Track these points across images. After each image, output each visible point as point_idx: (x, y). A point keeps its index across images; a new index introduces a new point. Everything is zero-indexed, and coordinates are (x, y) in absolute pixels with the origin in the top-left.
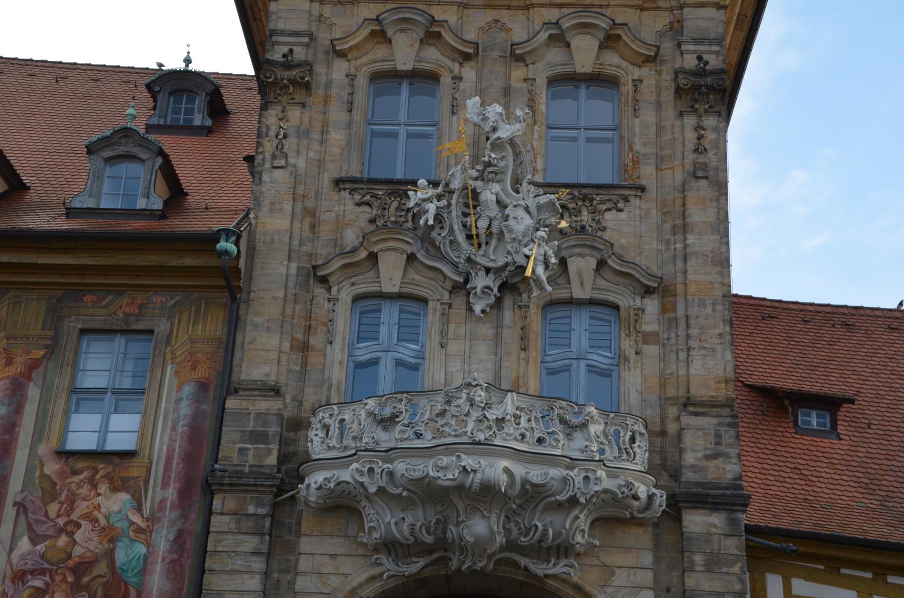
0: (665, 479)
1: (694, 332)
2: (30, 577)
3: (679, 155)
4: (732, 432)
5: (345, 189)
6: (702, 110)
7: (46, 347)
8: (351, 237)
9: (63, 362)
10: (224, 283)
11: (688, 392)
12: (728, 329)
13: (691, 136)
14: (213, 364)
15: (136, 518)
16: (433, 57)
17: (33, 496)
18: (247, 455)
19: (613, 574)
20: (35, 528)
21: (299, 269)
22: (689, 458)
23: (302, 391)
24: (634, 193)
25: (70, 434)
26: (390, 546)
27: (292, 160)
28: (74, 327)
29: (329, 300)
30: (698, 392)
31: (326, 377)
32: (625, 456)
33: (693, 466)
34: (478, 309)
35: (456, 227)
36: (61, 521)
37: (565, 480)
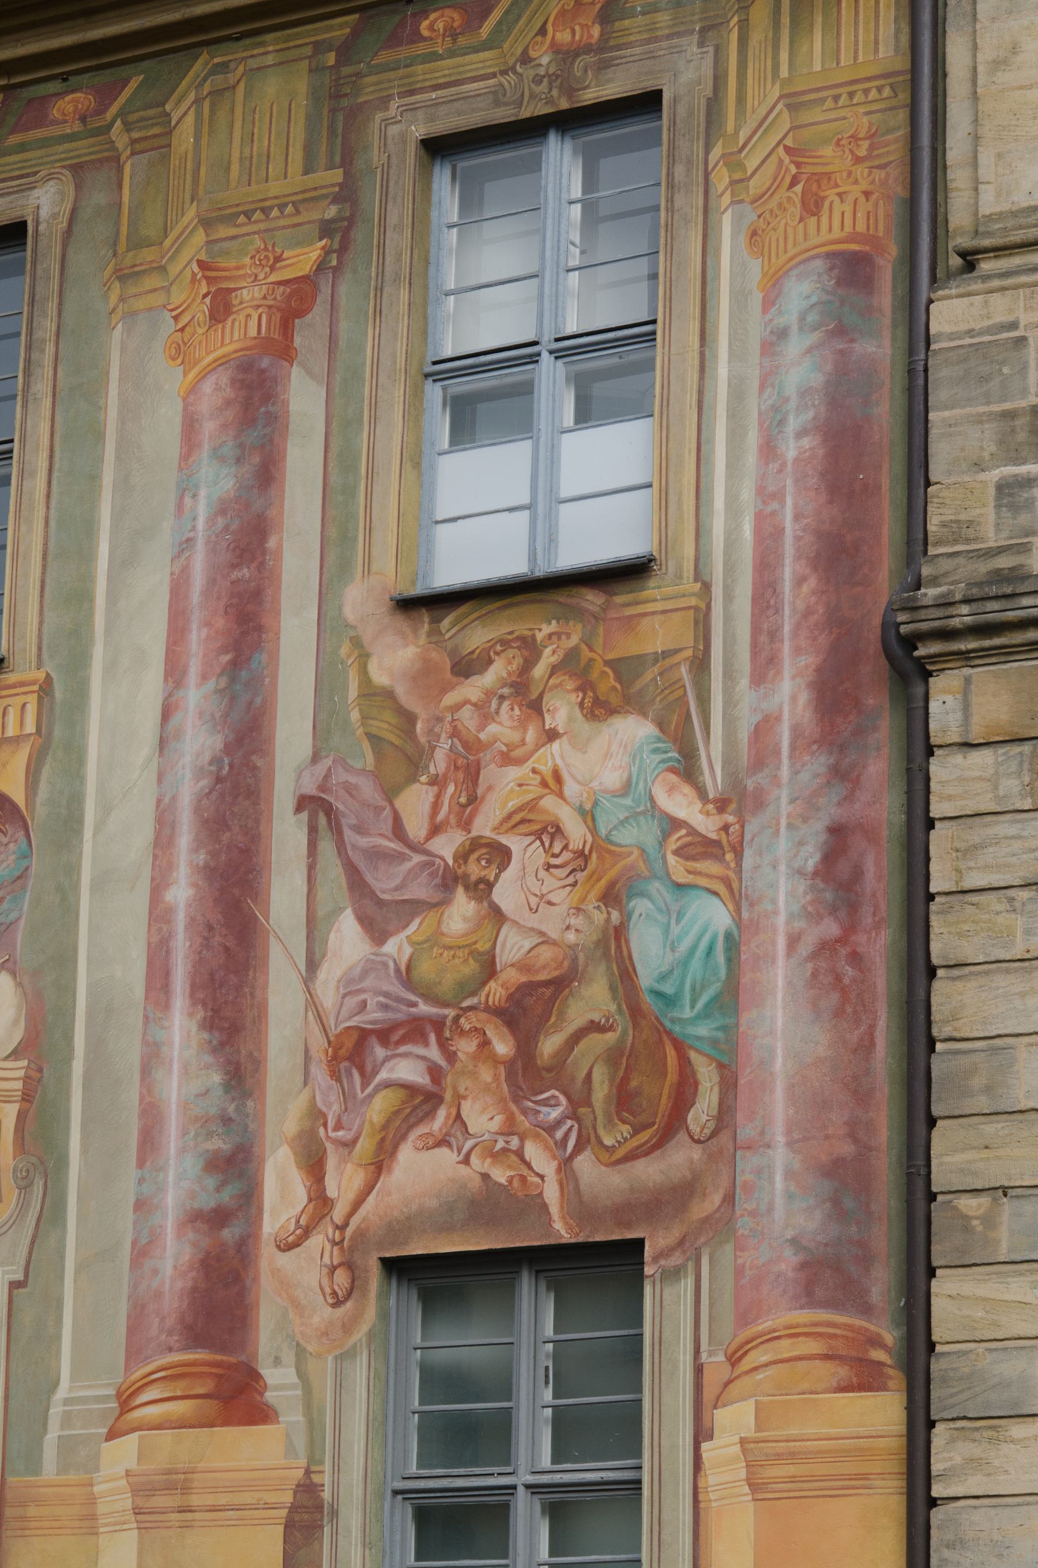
2: (380, 1052)
7: (326, 229)
9: (381, 273)
14: (879, 175)
15: (682, 805)
17: (348, 769)
20: (369, 878)
28: (403, 138)
36: (446, 847)
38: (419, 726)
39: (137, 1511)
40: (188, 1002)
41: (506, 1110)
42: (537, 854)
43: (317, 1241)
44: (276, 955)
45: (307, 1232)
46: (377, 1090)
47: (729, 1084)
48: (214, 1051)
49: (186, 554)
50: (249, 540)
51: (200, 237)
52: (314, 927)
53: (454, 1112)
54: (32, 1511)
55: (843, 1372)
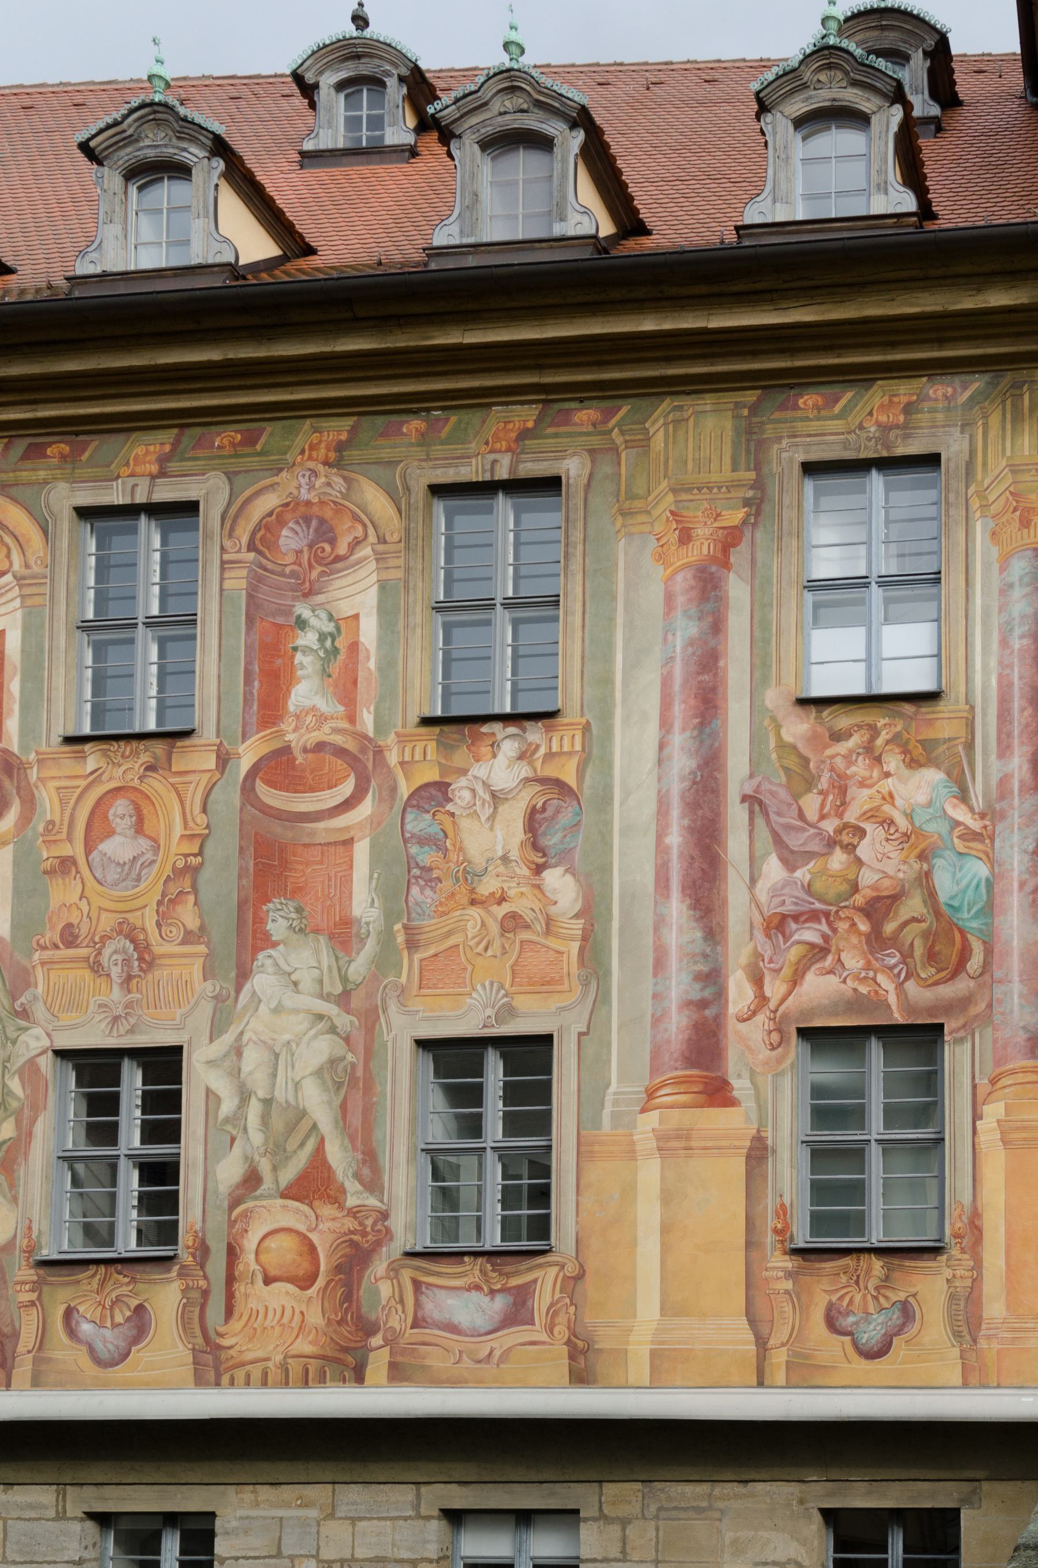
2: (794, 926)
17: (771, 783)
20: (785, 838)
36: (829, 826)
38: (811, 765)
39: (660, 1149)
40: (680, 895)
41: (866, 958)
42: (881, 833)
43: (760, 1018)
44: (731, 873)
45: (754, 1013)
46: (793, 944)
48: (697, 920)
49: (670, 665)
50: (708, 661)
51: (670, 498)
52: (754, 862)
53: (837, 957)
54: (596, 1148)
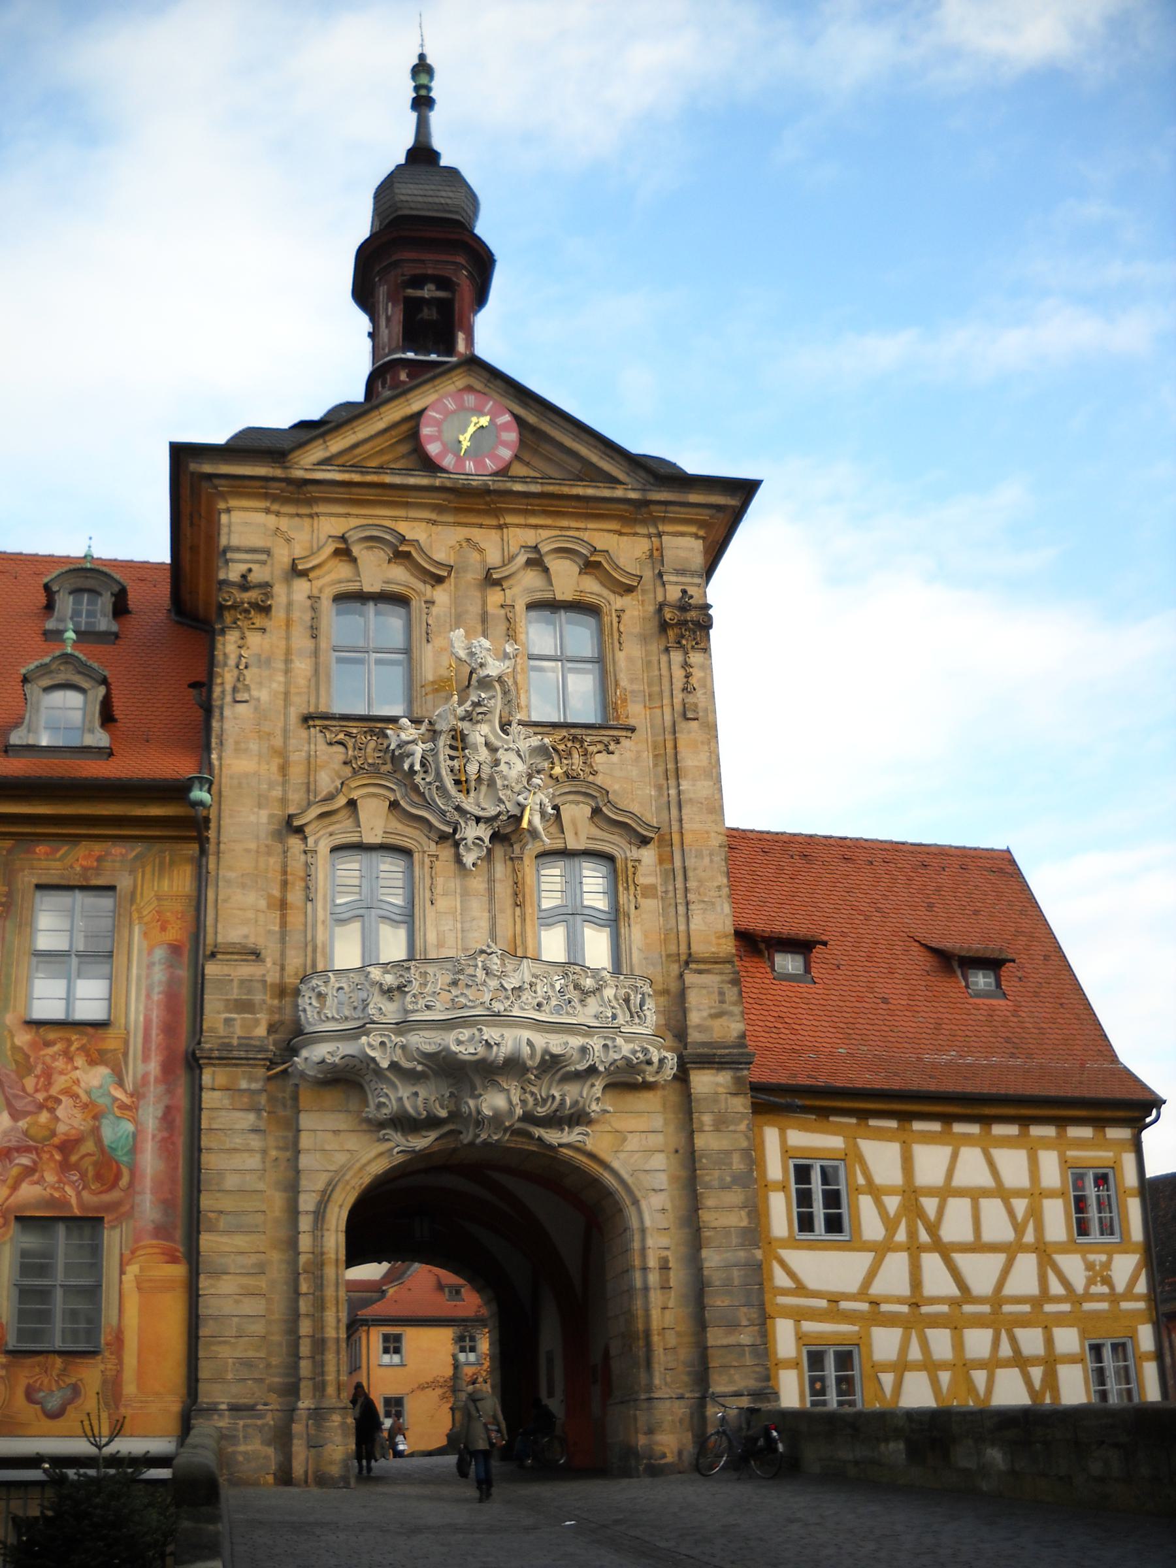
0: (670, 1041)
1: (692, 884)
2: (16, 1154)
3: (666, 694)
4: (735, 990)
5: (314, 726)
6: (689, 646)
8: (325, 782)
10: (195, 834)
11: (689, 948)
12: (725, 881)
13: (678, 674)
15: (119, 1094)
16: (398, 577)
18: (233, 1026)
19: (624, 1140)
21: (271, 816)
22: (694, 1018)
23: (283, 954)
24: (624, 734)
25: (35, 1001)
26: (404, 1123)
27: (255, 693)
29: (305, 852)
30: (698, 948)
31: (309, 938)
32: (637, 1020)
33: (699, 1028)
34: (469, 859)
35: (444, 773)
36: (40, 1097)
37: (584, 1050)
47: (133, 1174)
55: (166, 1258)
